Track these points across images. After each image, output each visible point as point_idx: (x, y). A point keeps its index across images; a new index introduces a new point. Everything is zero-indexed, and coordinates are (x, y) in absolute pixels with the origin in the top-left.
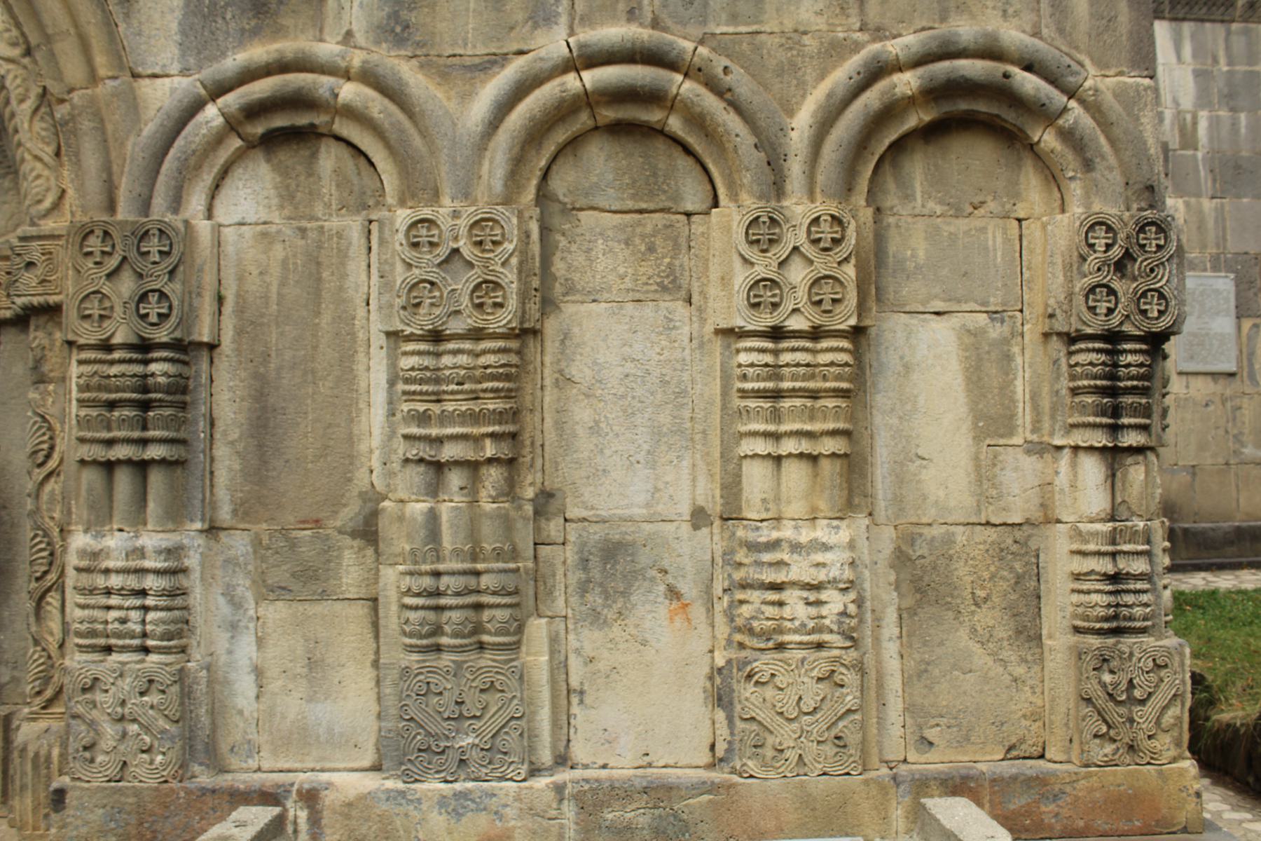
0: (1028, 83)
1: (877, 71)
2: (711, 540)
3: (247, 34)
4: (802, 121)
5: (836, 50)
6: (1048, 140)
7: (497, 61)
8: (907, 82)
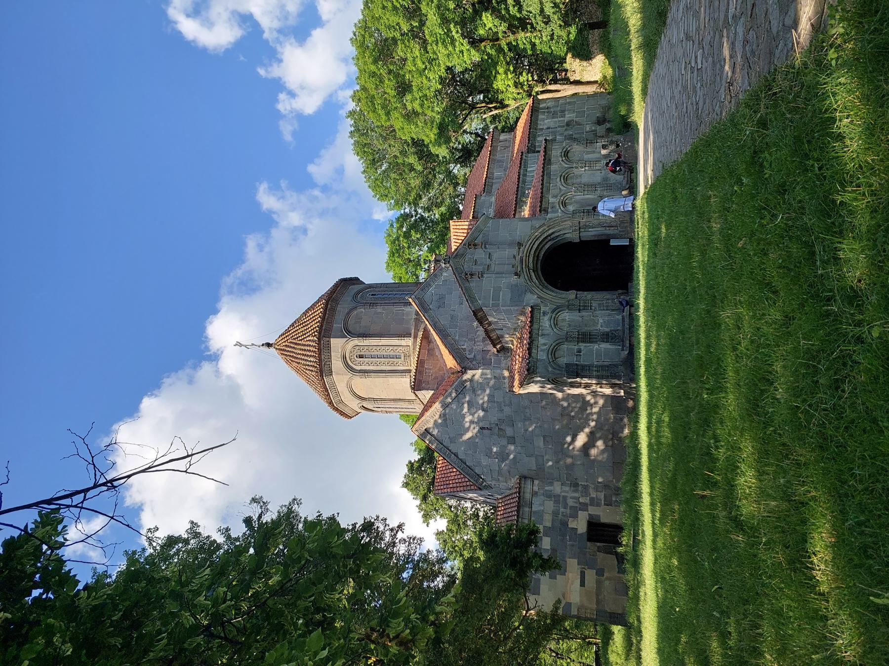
0: (564, 150)
1: (563, 160)
2: (603, 171)
3: (554, 209)
4: (566, 166)
5: (560, 163)
6: (569, 149)
7: (560, 188)
8: (564, 158)
